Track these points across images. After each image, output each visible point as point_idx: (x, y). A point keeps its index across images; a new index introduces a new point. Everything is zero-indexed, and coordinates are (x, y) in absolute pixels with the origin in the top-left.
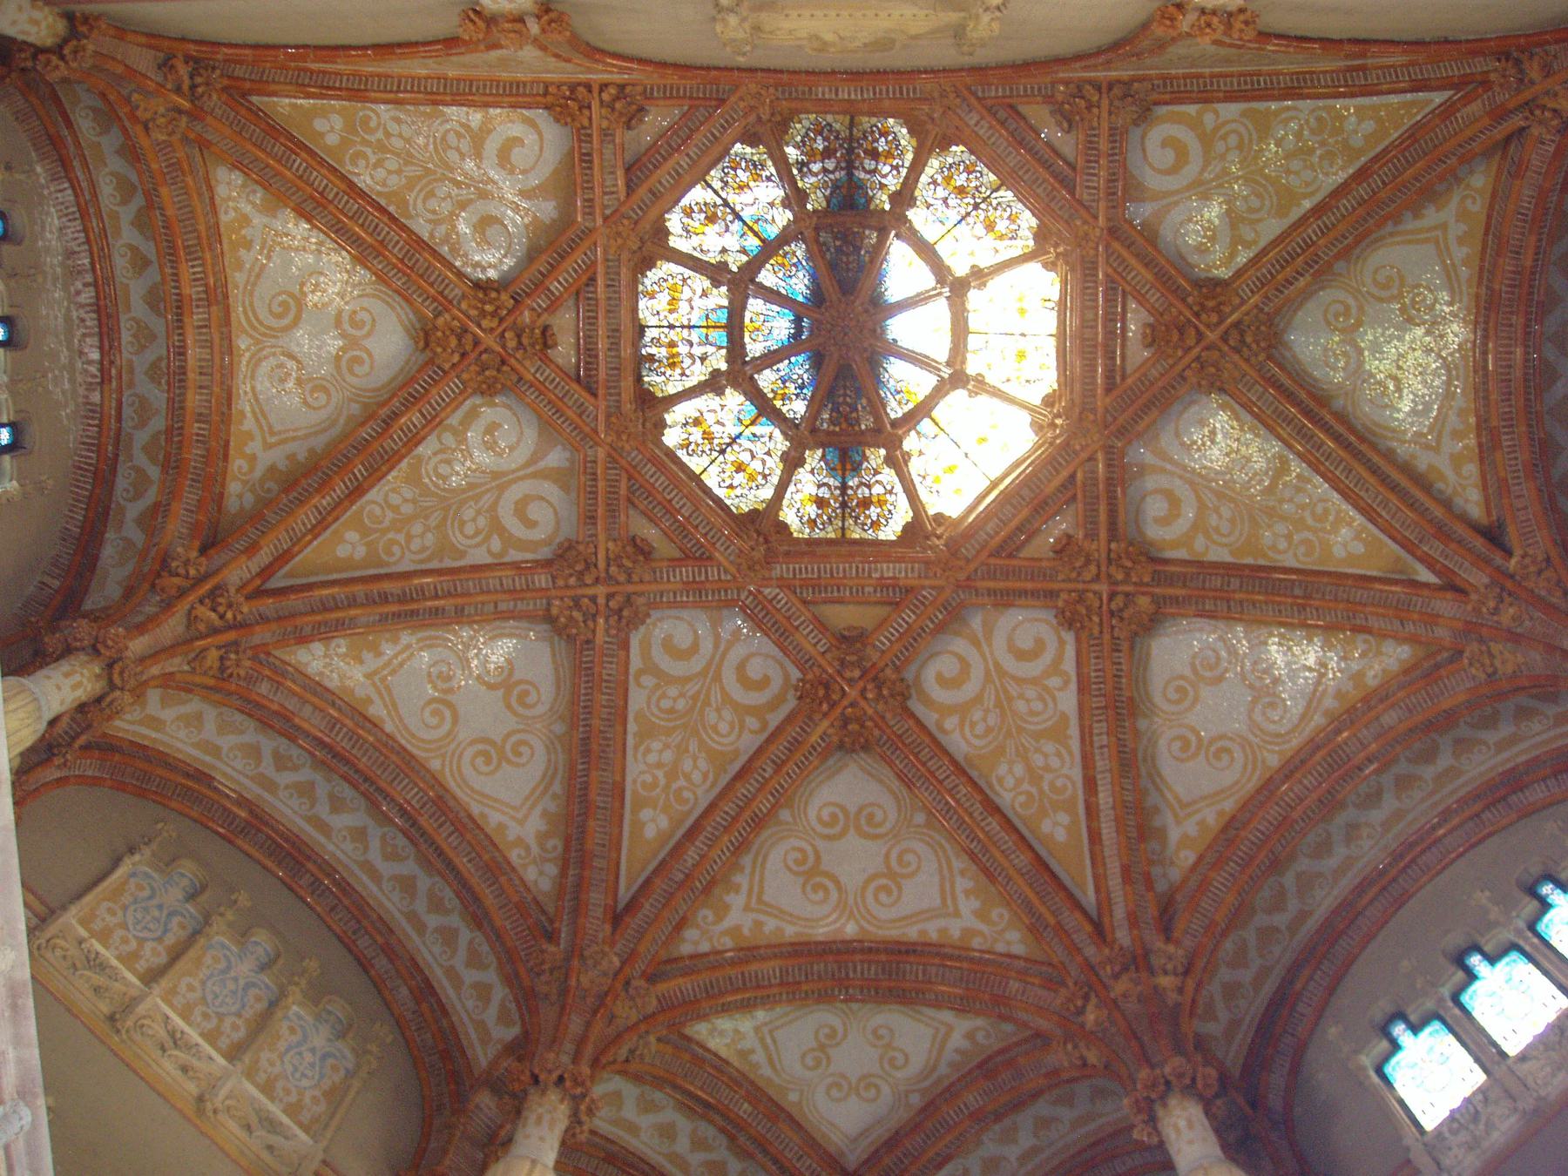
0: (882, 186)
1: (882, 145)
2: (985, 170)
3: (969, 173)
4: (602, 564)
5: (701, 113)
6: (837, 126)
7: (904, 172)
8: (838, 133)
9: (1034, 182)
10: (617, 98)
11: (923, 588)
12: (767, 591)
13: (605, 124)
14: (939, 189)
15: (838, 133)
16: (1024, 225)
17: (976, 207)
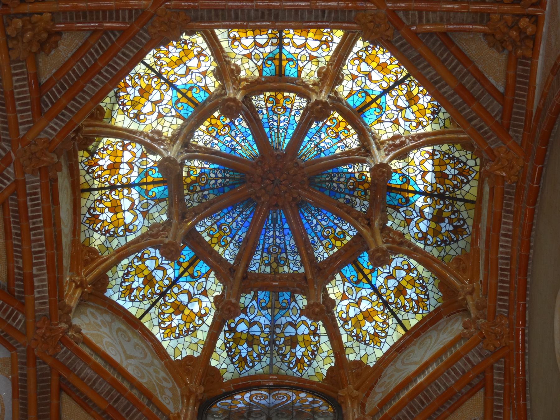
0: (408, 222)
1: (445, 226)
2: (419, 317)
3: (417, 302)
4: (27, 8)
5: (495, 107)
6: (466, 188)
7: (421, 245)
8: (460, 189)
9: (412, 408)
10: (521, 31)
11: (25, 314)
12: (11, 169)
13: (495, 17)
14: (403, 273)
15: (460, 189)
16: (370, 350)
17: (386, 304)
